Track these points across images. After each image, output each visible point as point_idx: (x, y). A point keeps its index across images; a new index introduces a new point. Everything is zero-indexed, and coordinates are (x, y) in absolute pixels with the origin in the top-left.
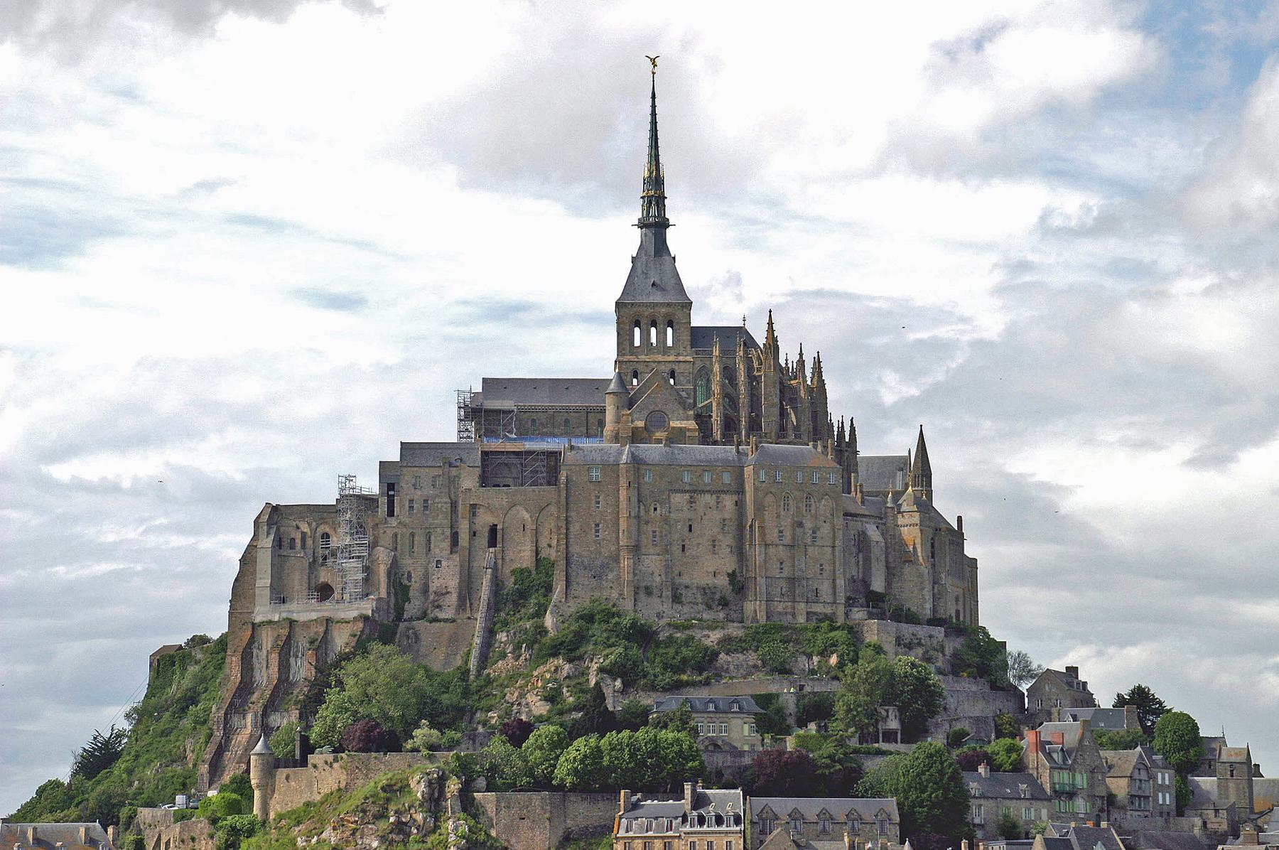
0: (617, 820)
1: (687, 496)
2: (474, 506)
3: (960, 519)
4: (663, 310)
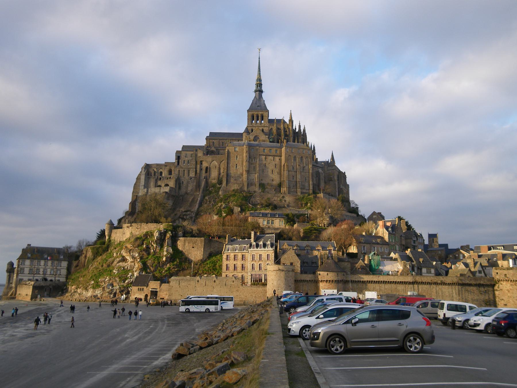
0: (224, 246)
1: (265, 157)
2: (201, 161)
3: (345, 172)
4: (261, 113)
